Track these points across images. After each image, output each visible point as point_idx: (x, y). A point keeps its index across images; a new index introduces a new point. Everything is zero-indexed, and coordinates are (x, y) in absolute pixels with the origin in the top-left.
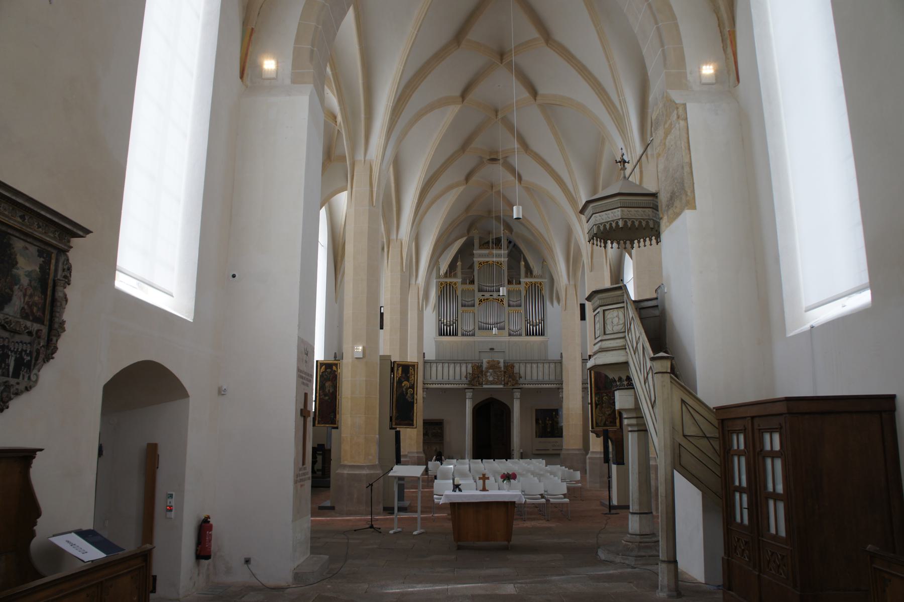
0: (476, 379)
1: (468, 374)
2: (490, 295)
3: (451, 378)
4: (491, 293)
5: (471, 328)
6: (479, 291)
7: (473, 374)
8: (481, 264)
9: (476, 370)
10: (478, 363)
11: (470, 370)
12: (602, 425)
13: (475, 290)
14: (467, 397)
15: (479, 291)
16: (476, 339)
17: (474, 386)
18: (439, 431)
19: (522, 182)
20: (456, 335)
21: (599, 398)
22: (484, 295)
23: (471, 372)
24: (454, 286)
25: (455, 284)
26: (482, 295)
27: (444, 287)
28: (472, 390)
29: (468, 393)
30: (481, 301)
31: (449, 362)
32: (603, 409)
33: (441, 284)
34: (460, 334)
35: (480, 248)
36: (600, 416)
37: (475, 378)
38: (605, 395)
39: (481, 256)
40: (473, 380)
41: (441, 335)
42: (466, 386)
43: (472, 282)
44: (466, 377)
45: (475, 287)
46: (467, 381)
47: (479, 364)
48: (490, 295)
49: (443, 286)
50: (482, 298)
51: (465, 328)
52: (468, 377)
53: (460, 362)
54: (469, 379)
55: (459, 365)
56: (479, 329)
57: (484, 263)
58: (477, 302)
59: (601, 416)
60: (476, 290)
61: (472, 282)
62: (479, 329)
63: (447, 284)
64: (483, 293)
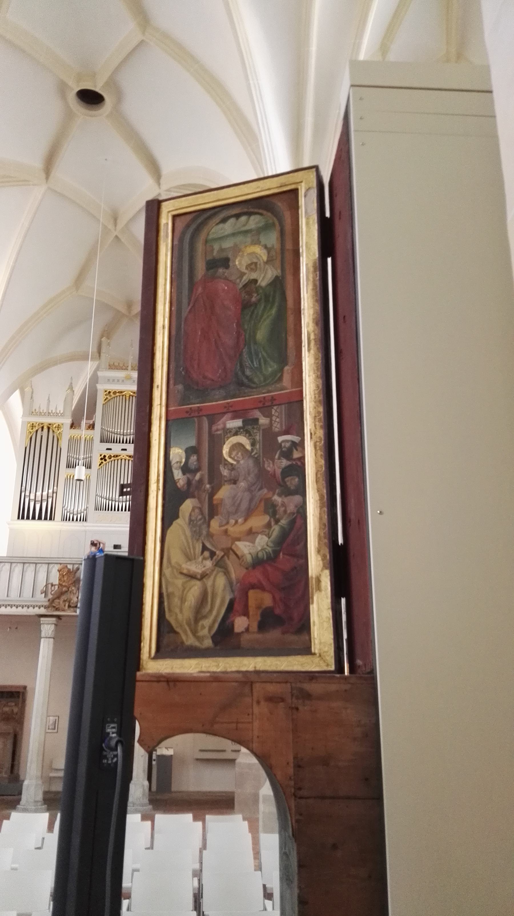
0: (64, 597)
1: (50, 586)
2: (123, 450)
3: (14, 595)
4: (124, 446)
5: (82, 507)
6: (102, 441)
7: (60, 585)
8: (110, 396)
9: (65, 579)
10: (73, 564)
11: (55, 579)
12: (208, 643)
13: (95, 438)
14: (43, 634)
15: (102, 441)
16: (87, 528)
17: (57, 609)
18: (16, 710)
19: (162, 181)
20: (51, 519)
21: (190, 451)
22: (110, 449)
23: (56, 582)
24: (56, 430)
25: (59, 427)
26: (108, 449)
27: (37, 431)
28: (54, 620)
29: (46, 626)
30: (104, 458)
31: (24, 563)
32: (215, 524)
33: (33, 426)
34: (58, 515)
35: (109, 369)
36: (192, 576)
37: (62, 593)
38: (238, 423)
39: (109, 381)
40: (58, 598)
41: (23, 518)
42: (42, 611)
43: (92, 427)
44: (45, 592)
45: (96, 434)
46: (46, 599)
47: (76, 566)
48: (123, 450)
49: (35, 430)
50: (108, 453)
51: (70, 507)
52: (50, 591)
53: (36, 562)
54: (50, 596)
55: (33, 566)
56: (96, 509)
57: (115, 393)
58: (96, 461)
59: (204, 576)
60: (97, 439)
61: (92, 427)
62: (96, 509)
63: (43, 428)
64: (109, 445)
